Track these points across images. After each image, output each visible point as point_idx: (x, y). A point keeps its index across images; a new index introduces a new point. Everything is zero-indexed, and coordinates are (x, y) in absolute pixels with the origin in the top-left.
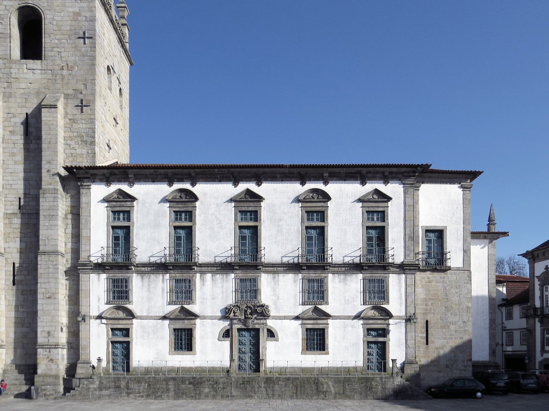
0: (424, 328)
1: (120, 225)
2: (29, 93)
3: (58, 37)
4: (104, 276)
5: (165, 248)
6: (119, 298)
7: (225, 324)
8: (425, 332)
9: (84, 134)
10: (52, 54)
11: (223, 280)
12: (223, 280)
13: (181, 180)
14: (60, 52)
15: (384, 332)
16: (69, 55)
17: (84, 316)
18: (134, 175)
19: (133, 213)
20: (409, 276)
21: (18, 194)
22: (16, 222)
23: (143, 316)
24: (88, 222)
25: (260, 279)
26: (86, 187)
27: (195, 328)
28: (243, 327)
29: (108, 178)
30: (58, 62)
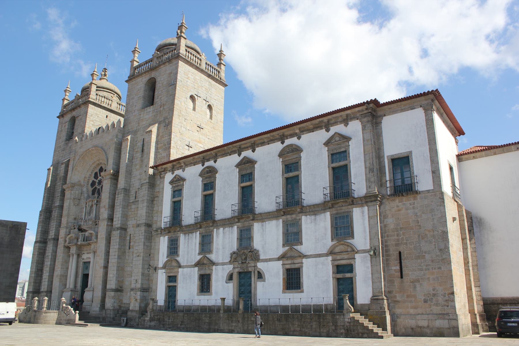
0: (397, 260)
4: (166, 237)
7: (231, 267)
8: (399, 264)
9: (166, 144)
11: (230, 232)
12: (230, 232)
13: (208, 160)
15: (350, 268)
17: (156, 267)
18: (184, 163)
20: (372, 208)
24: (162, 201)
25: (253, 228)
27: (212, 273)
28: (241, 271)
30: (160, 104)
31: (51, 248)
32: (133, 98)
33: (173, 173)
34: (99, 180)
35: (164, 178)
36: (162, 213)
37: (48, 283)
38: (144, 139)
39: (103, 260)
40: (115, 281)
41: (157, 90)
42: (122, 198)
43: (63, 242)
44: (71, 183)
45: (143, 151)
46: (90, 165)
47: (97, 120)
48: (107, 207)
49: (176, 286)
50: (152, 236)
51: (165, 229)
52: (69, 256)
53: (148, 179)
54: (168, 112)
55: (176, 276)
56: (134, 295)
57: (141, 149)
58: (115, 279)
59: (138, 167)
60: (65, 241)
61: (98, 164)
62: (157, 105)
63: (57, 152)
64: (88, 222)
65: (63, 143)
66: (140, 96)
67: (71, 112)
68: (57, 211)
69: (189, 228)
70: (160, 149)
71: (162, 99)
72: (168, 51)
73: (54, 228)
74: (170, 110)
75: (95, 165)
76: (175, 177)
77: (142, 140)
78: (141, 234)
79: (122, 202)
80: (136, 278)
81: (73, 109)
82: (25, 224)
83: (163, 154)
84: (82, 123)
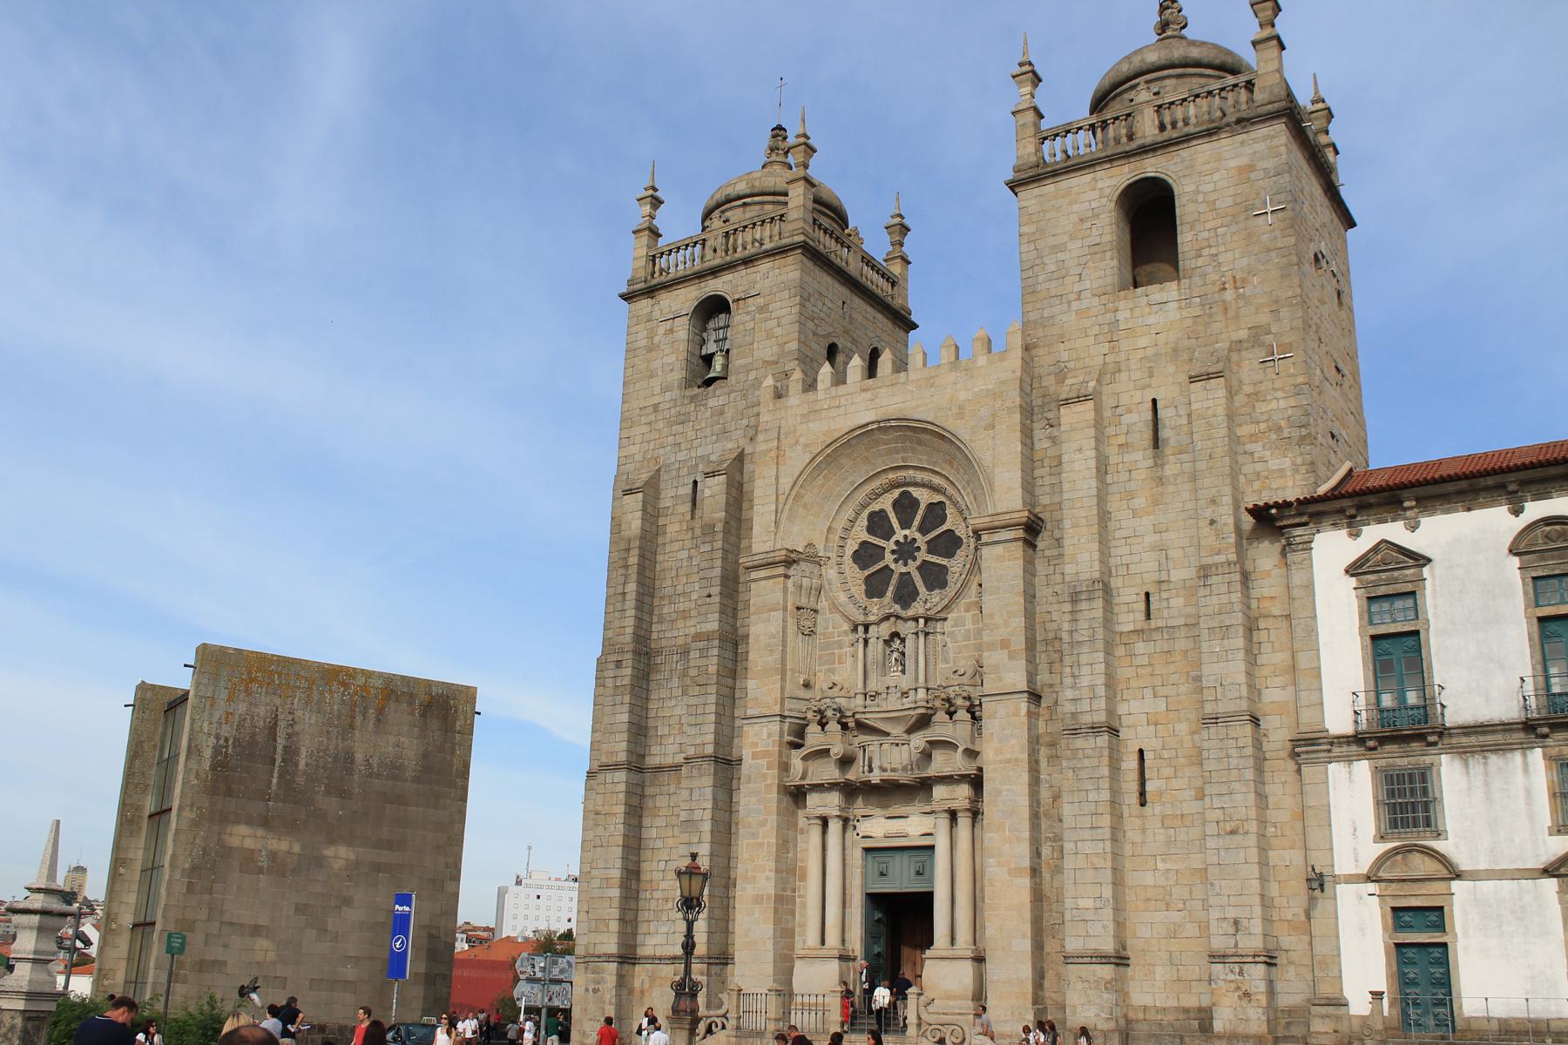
1: (1392, 631)
2: (1156, 354)
3: (1208, 226)
4: (1363, 770)
5: (1522, 678)
6: (1406, 824)
9: (1283, 423)
14: (1216, 255)
16: (1236, 256)
19: (1424, 595)
21: (1144, 583)
23: (1478, 871)
24: (1312, 631)
26: (1301, 546)
29: (1353, 517)
30: (1213, 277)
31: (709, 792)
32: (1061, 248)
33: (1355, 535)
34: (897, 542)
35: (1307, 546)
36: (1319, 676)
37: (709, 926)
38: (1154, 401)
39: (1027, 843)
40: (1111, 925)
41: (1186, 227)
42: (1099, 613)
43: (776, 771)
44: (787, 550)
45: (1156, 442)
46: (852, 483)
47: (822, 315)
48: (1019, 642)
49: (1444, 945)
50: (1265, 759)
51: (1358, 739)
53: (1234, 550)
54: (1266, 310)
55: (1441, 909)
56: (1231, 977)
57: (1148, 434)
58: (1111, 917)
59: (1140, 502)
60: (785, 767)
62: (1196, 279)
63: (645, 429)
64: (884, 696)
65: (676, 393)
67: (697, 281)
68: (715, 651)
69: (1484, 733)
70: (1251, 442)
71: (1221, 259)
72: (1215, 85)
73: (712, 718)
76: (1375, 549)
78: (1233, 752)
79: (1101, 631)
80: (1231, 913)
81: (715, 272)
82: (469, 694)
84: (773, 323)
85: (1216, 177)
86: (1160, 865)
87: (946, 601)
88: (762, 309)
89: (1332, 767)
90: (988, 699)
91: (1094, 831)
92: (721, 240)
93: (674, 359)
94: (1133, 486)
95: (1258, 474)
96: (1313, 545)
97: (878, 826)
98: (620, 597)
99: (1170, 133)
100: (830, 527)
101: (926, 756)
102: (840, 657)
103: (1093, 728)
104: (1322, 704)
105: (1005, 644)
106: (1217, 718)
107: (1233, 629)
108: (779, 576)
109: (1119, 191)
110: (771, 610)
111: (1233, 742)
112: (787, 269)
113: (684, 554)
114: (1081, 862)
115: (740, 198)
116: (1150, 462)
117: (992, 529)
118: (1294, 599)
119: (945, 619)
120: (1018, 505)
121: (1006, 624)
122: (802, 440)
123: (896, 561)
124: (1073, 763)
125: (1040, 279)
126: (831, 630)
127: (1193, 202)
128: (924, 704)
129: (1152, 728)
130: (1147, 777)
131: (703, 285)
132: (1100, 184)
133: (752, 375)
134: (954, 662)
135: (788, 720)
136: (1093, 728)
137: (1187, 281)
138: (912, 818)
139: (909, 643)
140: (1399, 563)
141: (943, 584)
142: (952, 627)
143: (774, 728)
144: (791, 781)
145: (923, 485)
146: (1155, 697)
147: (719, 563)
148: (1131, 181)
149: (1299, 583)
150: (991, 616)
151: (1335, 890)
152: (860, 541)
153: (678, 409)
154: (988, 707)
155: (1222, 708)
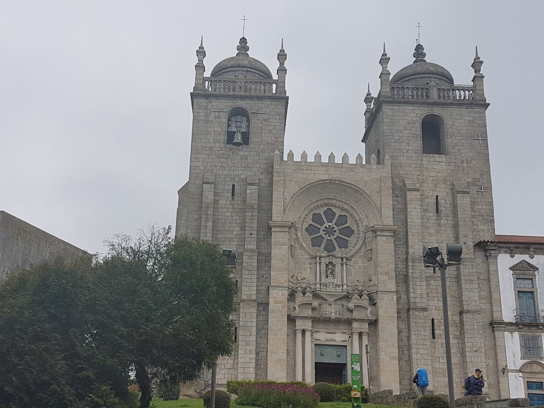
3: (457, 138)
4: (516, 334)
9: (484, 214)
10: (454, 151)
14: (460, 149)
22: (433, 284)
26: (493, 257)
38: (437, 196)
41: (449, 136)
51: (516, 324)
52: (295, 332)
57: (435, 208)
59: (432, 231)
61: (326, 205)
63: (205, 156)
64: (328, 286)
65: (222, 145)
66: (413, 132)
74: (482, 171)
75: (319, 203)
76: (520, 263)
77: (436, 197)
78: (476, 324)
81: (242, 98)
83: (480, 226)
85: (460, 121)
86: (441, 361)
87: (351, 254)
88: (266, 120)
89: (506, 333)
90: (381, 293)
91: (424, 346)
92: (243, 84)
93: (220, 130)
94: (429, 224)
95: (475, 229)
96: (498, 257)
97: (323, 336)
98: (203, 227)
99: (442, 100)
100: (300, 216)
101: (351, 311)
102: (304, 268)
103: (422, 309)
104: (501, 311)
105: (387, 273)
106: (469, 311)
107: (474, 281)
108: (287, 232)
109: (423, 116)
110: (282, 245)
111: (475, 320)
112: (279, 107)
113: (230, 214)
114: (419, 356)
115: (244, 67)
116: (436, 218)
117: (383, 230)
118: (491, 275)
119: (351, 260)
120: (392, 223)
121: (388, 267)
122: (294, 180)
123: (325, 234)
124: (414, 320)
125: (392, 141)
126: (300, 257)
127: (452, 128)
128: (346, 291)
129: (437, 311)
130: (436, 327)
131: (235, 101)
132: (416, 112)
133: (262, 147)
134: (354, 277)
135: (290, 290)
136: (422, 309)
137: (449, 156)
138: (336, 335)
139: (338, 268)
140: (527, 268)
141: (346, 247)
142: (353, 263)
143: (285, 292)
144: (294, 314)
145: (338, 207)
146: (438, 301)
147: (256, 221)
148: (428, 114)
149: (493, 269)
150: (382, 263)
151: (508, 374)
152: (309, 224)
153: (223, 152)
154: (380, 295)
155: (470, 308)
